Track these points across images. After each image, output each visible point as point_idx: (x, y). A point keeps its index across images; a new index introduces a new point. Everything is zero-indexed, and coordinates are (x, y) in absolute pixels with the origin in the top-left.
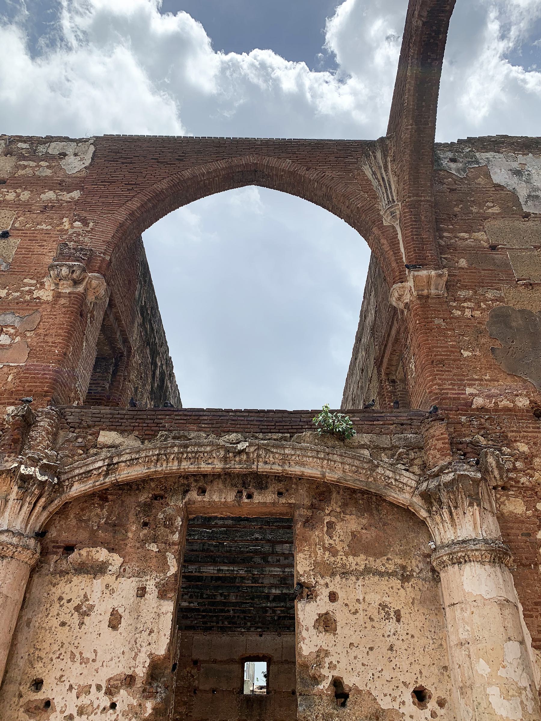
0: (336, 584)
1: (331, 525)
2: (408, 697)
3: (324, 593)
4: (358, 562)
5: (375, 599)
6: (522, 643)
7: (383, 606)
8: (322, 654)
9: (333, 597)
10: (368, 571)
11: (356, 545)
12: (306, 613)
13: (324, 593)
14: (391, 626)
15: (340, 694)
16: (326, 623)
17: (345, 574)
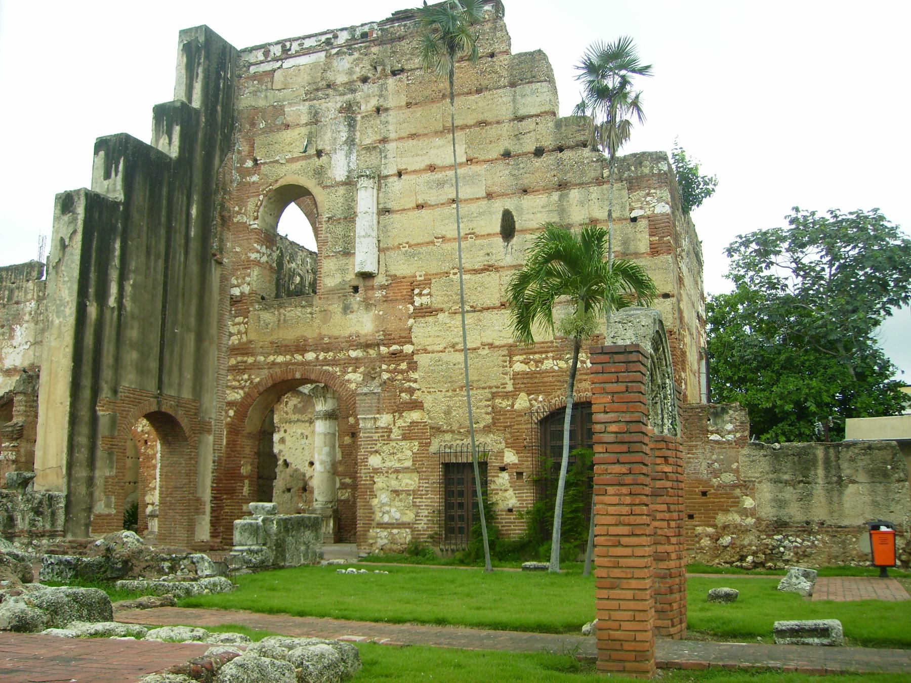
0: (287, 426)
1: (287, 403)
2: (307, 463)
3: (282, 430)
4: (294, 417)
5: (299, 431)
6: (334, 446)
7: (302, 434)
8: (281, 451)
9: (285, 431)
10: (298, 420)
11: (296, 410)
12: (276, 437)
13: (282, 430)
14: (304, 441)
15: (286, 464)
16: (282, 440)
17: (290, 422)
